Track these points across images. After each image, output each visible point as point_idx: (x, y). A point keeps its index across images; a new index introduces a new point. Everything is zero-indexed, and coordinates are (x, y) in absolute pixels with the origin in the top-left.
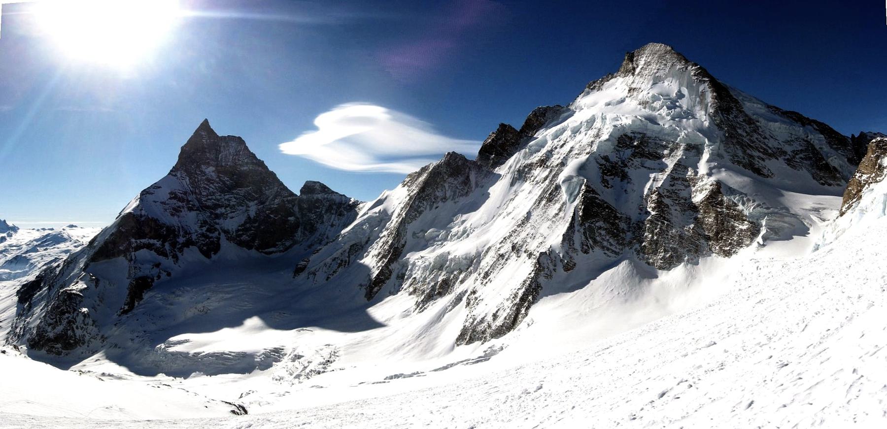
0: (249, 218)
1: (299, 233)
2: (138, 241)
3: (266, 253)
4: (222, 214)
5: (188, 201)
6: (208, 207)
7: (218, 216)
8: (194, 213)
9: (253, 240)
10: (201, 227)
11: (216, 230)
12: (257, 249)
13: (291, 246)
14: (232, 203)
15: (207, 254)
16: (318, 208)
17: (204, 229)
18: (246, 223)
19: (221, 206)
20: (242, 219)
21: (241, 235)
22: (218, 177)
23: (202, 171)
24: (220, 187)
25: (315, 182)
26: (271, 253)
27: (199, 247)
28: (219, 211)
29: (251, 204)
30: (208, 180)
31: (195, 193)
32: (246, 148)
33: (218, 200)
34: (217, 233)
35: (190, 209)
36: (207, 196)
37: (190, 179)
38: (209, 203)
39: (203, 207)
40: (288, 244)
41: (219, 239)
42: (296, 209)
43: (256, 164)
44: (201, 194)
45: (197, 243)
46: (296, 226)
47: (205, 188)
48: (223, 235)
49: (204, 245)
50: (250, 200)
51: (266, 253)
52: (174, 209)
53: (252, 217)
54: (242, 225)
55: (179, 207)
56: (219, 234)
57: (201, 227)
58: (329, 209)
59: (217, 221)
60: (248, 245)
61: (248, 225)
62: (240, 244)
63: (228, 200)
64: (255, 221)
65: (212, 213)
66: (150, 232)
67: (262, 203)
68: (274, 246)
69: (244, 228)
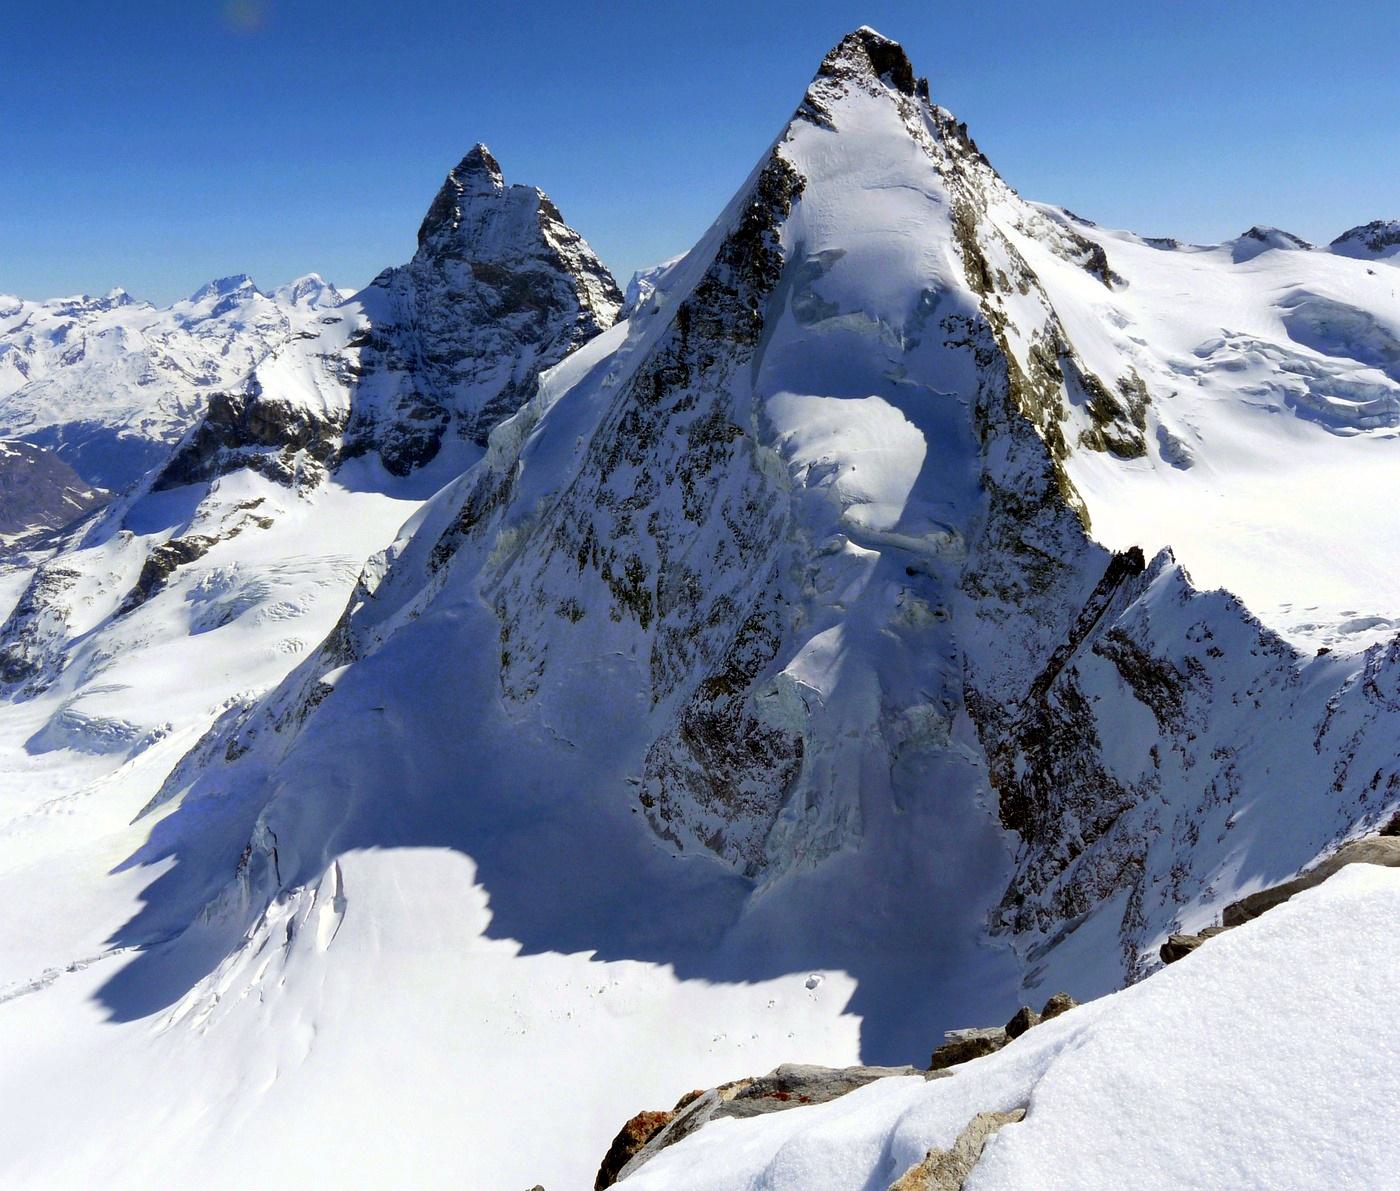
2: (234, 451)
4: (465, 374)
6: (437, 359)
7: (454, 378)
14: (491, 347)
19: (463, 355)
23: (443, 275)
24: (474, 312)
28: (465, 364)
33: (464, 342)
36: (442, 332)
38: (443, 349)
41: (439, 431)
43: (545, 258)
45: (382, 443)
49: (395, 448)
53: (518, 382)
54: (492, 402)
57: (401, 407)
63: (486, 341)
65: (444, 371)
66: (263, 431)
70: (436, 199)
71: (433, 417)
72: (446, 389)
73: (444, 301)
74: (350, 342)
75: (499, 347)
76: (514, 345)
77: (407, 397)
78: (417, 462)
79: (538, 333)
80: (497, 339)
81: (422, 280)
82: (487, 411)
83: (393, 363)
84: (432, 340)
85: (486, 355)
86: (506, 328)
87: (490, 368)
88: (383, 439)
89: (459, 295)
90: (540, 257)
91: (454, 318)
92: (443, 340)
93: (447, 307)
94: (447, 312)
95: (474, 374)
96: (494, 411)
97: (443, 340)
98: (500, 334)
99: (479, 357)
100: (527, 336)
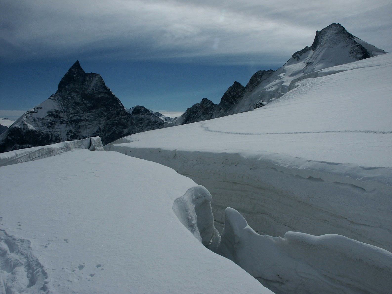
4: (83, 126)
8: (64, 125)
22: (82, 101)
23: (72, 97)
25: (141, 107)
28: (82, 124)
29: (101, 119)
30: (76, 103)
31: (66, 112)
36: (74, 113)
38: (75, 118)
50: (101, 117)
52: (50, 123)
55: (54, 121)
63: (88, 116)
70: (65, 75)
73: (74, 104)
74: (47, 115)
77: (68, 131)
79: (105, 114)
81: (65, 98)
83: (61, 121)
86: (94, 113)
89: (78, 103)
90: (105, 93)
91: (77, 109)
92: (75, 116)
97: (75, 116)
98: (92, 115)
100: (102, 115)
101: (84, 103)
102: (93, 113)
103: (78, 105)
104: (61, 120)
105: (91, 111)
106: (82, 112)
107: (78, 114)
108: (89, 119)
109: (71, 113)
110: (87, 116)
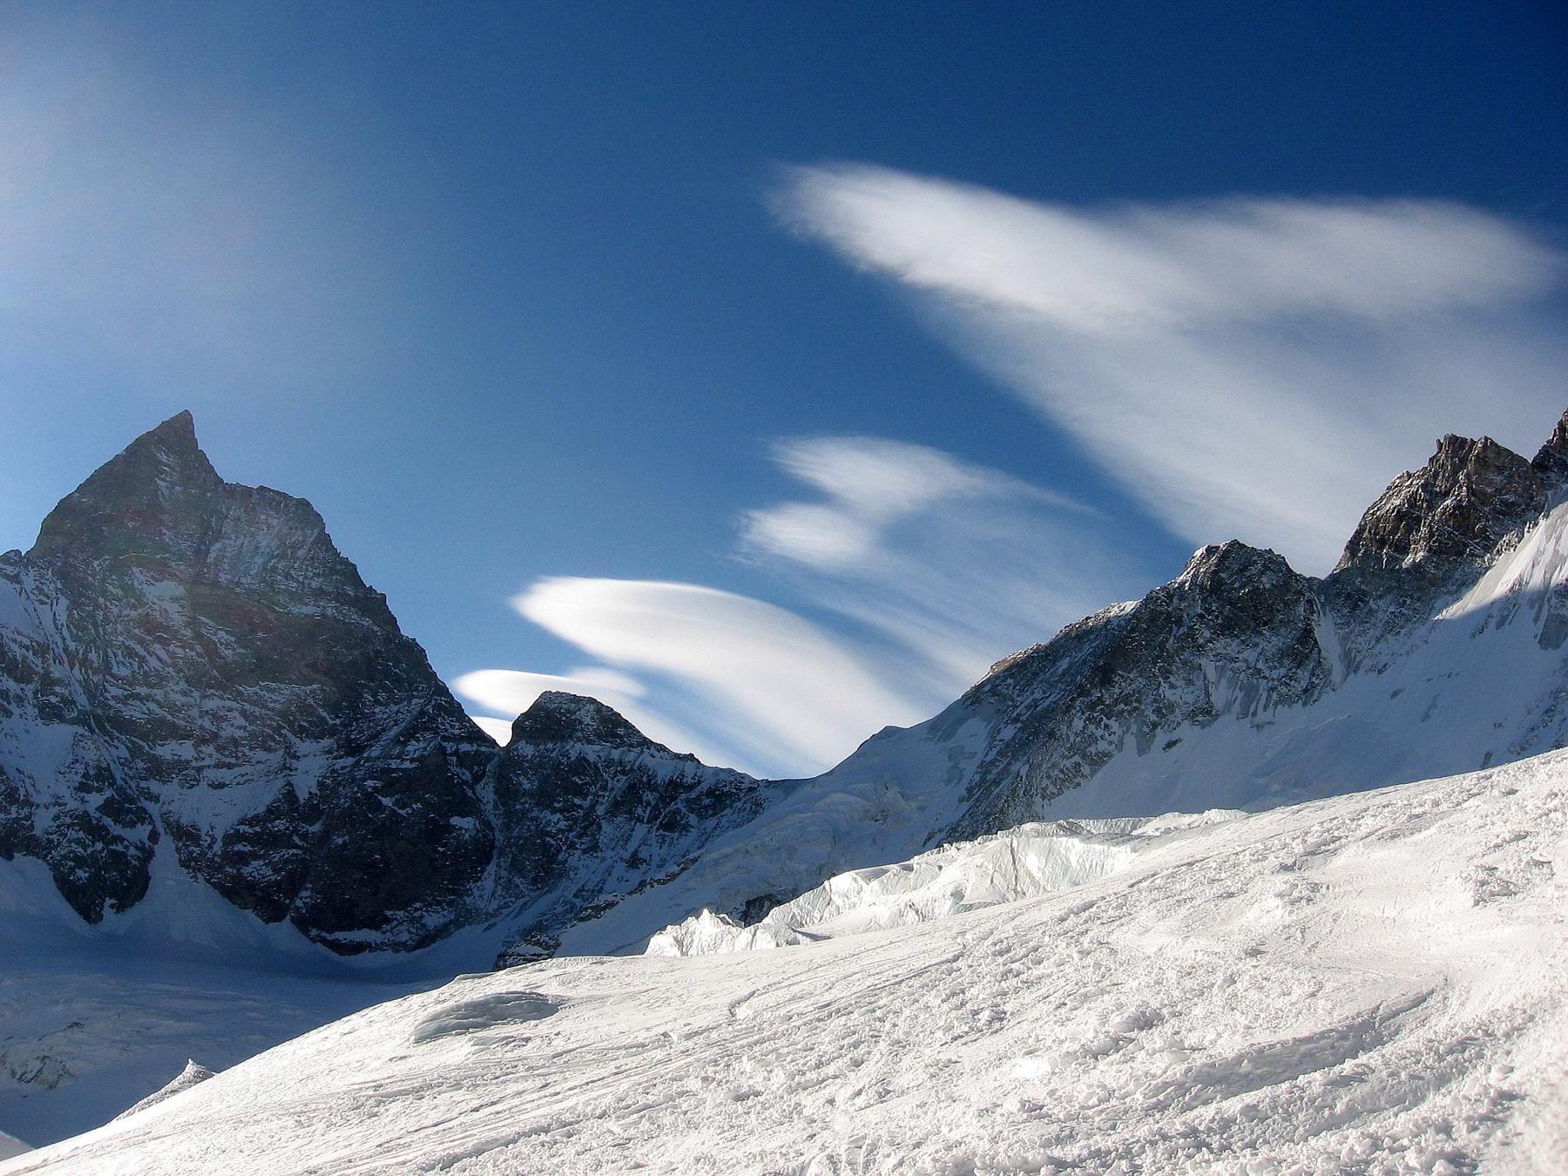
0: (290, 794)
1: (488, 883)
3: (336, 946)
4: (180, 765)
5: (48, 683)
6: (124, 725)
7: (158, 769)
8: (62, 733)
9: (292, 885)
10: (83, 788)
11: (142, 816)
12: (302, 924)
13: (443, 932)
14: (227, 731)
15: (84, 900)
16: (580, 791)
17: (95, 800)
18: (272, 812)
20: (262, 796)
21: (243, 859)
22: (193, 622)
23: (128, 589)
25: (575, 699)
26: (358, 948)
27: (55, 867)
29: (305, 746)
31: (85, 663)
32: (325, 541)
33: (174, 709)
34: (142, 832)
35: (51, 713)
37: (75, 605)
38: (134, 712)
39: (103, 722)
40: (433, 920)
41: (148, 855)
42: (486, 792)
44: (107, 667)
45: (50, 845)
46: (481, 852)
47: (131, 653)
48: (166, 848)
49: (80, 862)
50: (302, 732)
51: (336, 946)
53: (303, 796)
54: (256, 820)
56: (154, 836)
57: (83, 788)
58: (626, 803)
59: (154, 786)
60: (268, 903)
61: (280, 825)
62: (237, 891)
63: (215, 717)
64: (311, 812)
65: (135, 752)
67: (354, 749)
68: (376, 922)
69: (260, 834)
71: (132, 825)
72: (143, 784)
75: (241, 733)
76: (280, 735)
78: (114, 901)
80: (241, 721)
82: (237, 837)
84: (114, 691)
85: (220, 742)
86: (252, 703)
87: (229, 766)
88: (54, 837)
89: (167, 629)
92: (137, 697)
93: (141, 642)
94: (142, 652)
95: (199, 770)
96: (253, 839)
98: (243, 713)
99: (205, 741)
101: (198, 636)
102: (247, 706)
103: (160, 640)
104: (53, 699)
105: (240, 693)
106: (183, 685)
107: (158, 694)
108: (223, 734)
109: (112, 676)
110: (214, 715)
